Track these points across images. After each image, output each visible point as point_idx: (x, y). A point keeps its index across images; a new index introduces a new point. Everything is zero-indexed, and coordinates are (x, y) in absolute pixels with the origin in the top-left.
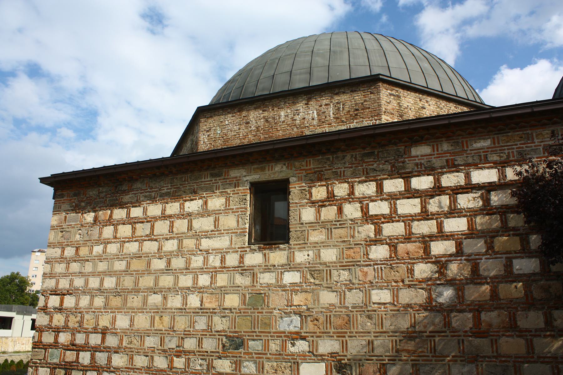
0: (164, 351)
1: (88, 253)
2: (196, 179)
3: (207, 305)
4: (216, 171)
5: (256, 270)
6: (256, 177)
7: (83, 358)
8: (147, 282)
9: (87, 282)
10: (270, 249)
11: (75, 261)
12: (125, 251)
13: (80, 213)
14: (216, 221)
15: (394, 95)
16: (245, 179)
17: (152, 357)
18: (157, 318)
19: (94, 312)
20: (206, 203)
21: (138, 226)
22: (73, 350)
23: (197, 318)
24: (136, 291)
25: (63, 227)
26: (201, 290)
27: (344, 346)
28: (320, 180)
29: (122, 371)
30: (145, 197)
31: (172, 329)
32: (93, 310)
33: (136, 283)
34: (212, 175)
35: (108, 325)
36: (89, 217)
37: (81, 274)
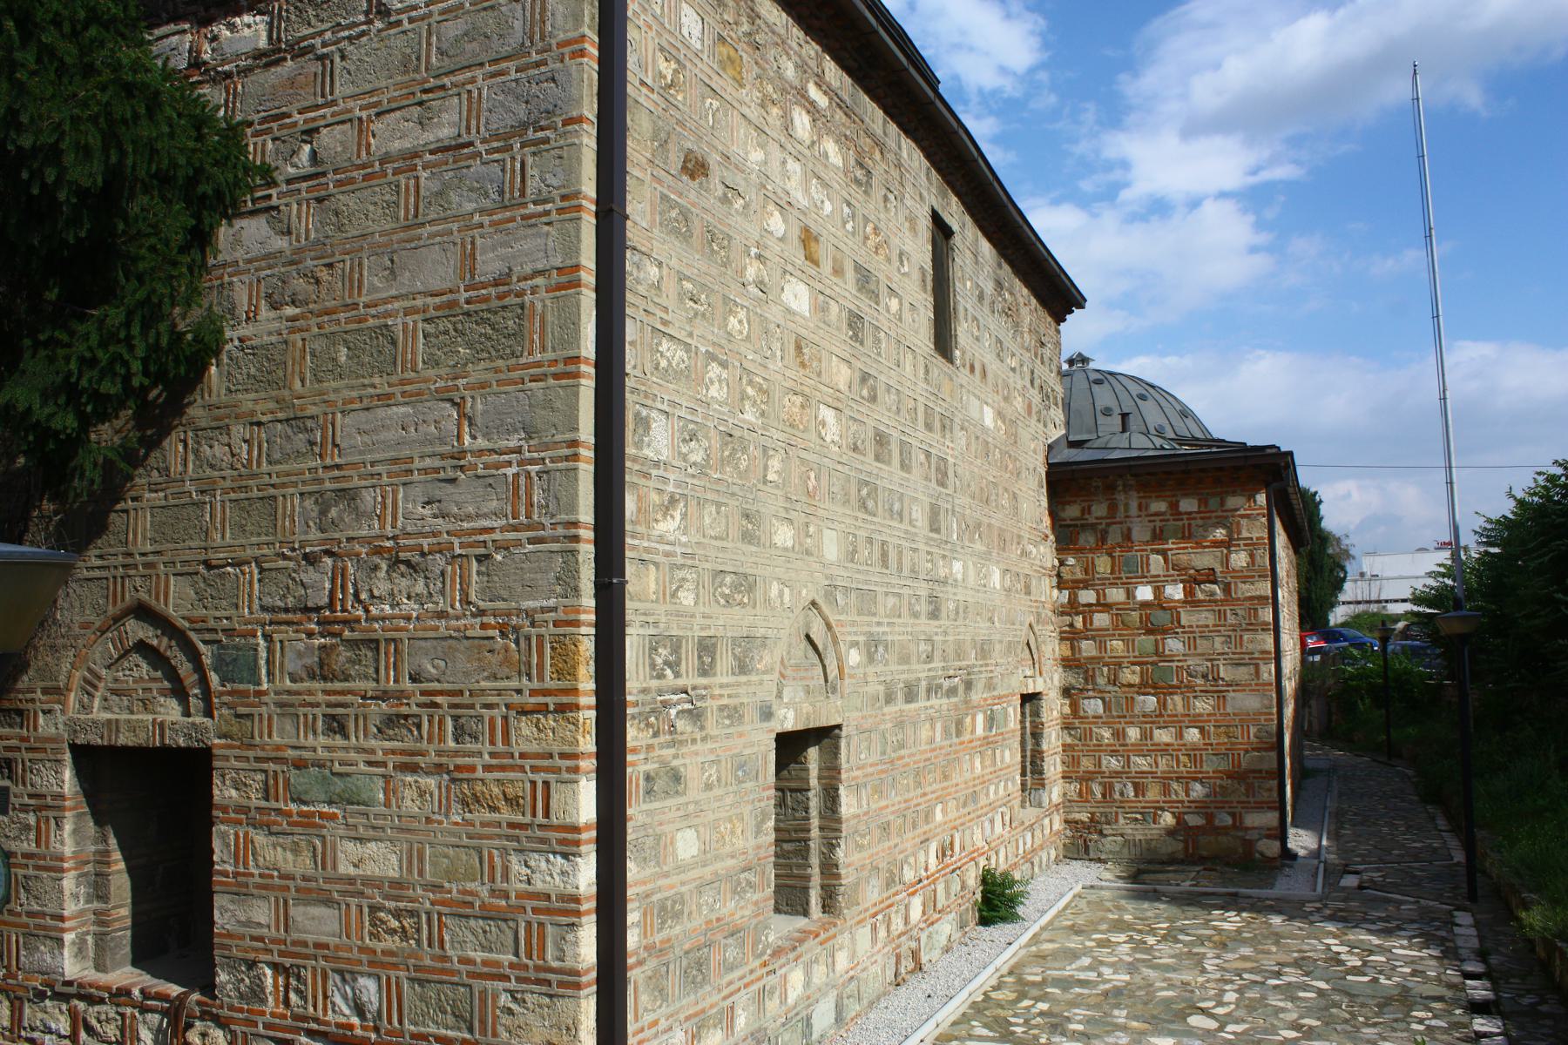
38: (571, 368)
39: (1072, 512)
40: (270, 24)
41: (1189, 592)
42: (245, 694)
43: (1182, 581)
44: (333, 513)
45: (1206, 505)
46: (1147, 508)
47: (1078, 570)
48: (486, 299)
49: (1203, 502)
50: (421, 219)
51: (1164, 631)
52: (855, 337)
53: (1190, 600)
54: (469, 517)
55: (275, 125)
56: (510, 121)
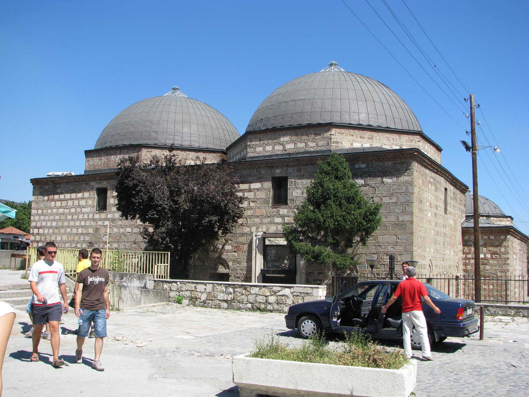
1: (46, 212)
3: (84, 232)
5: (97, 220)
6: (98, 186)
8: (66, 223)
9: (47, 224)
10: (101, 213)
11: (42, 215)
14: (86, 201)
15: (149, 151)
18: (69, 237)
20: (83, 194)
24: (63, 227)
26: (82, 227)
27: (119, 245)
30: (65, 191)
33: (63, 224)
34: (86, 184)
36: (46, 198)
38: (412, 233)
39: (466, 237)
40: (365, 180)
41: (491, 256)
42: (363, 271)
43: (490, 254)
44: (378, 248)
45: (496, 237)
46: (483, 238)
47: (467, 250)
48: (401, 223)
49: (495, 237)
50: (390, 212)
51: (486, 264)
52: (435, 217)
53: (492, 258)
54: (398, 250)
55: (366, 195)
56: (403, 201)
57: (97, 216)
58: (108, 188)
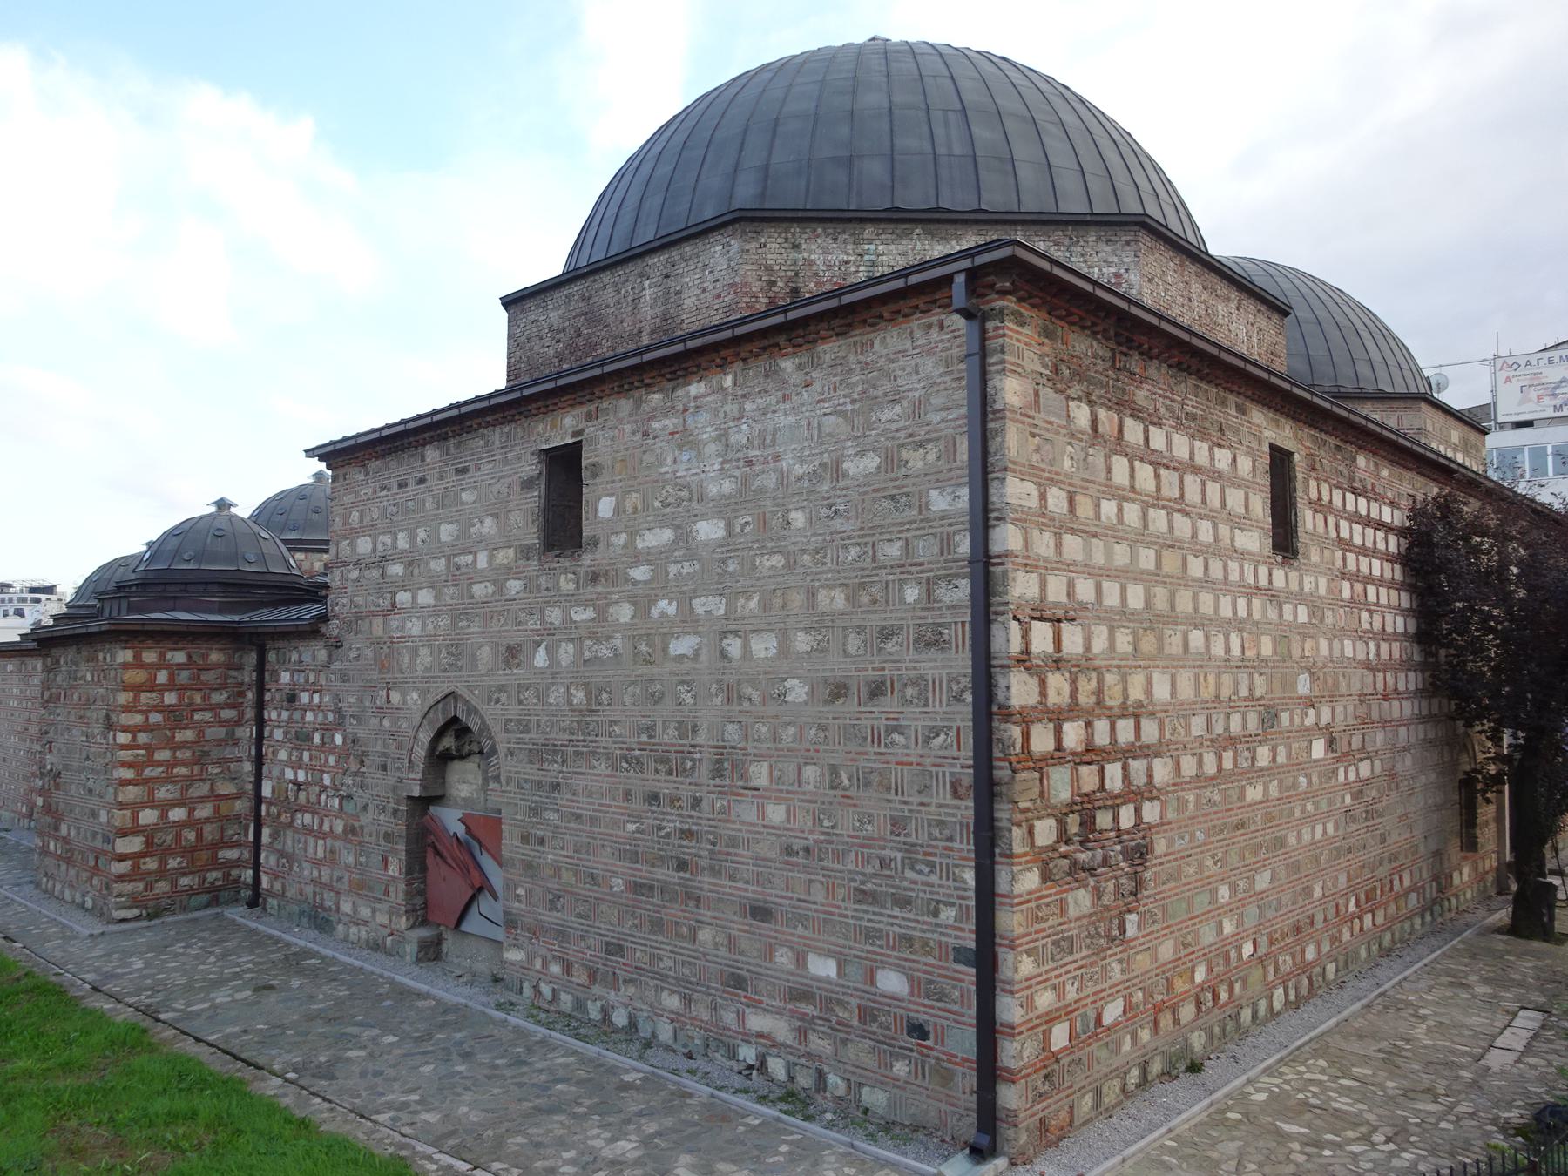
0: (1211, 740)
2: (1223, 403)
4: (1240, 400)
7: (1111, 779)
11: (1073, 531)
12: (1151, 528)
13: (1062, 392)
16: (1267, 433)
17: (1201, 755)
18: (1202, 678)
19: (1119, 667)
21: (1163, 472)
22: (1089, 763)
23: (1240, 675)
24: (1173, 619)
25: (1036, 422)
28: (1314, 469)
29: (1168, 792)
31: (1217, 697)
32: (1116, 662)
35: (1142, 697)
36: (1081, 415)
37: (1089, 570)
57: (1279, 575)
58: (1297, 457)
